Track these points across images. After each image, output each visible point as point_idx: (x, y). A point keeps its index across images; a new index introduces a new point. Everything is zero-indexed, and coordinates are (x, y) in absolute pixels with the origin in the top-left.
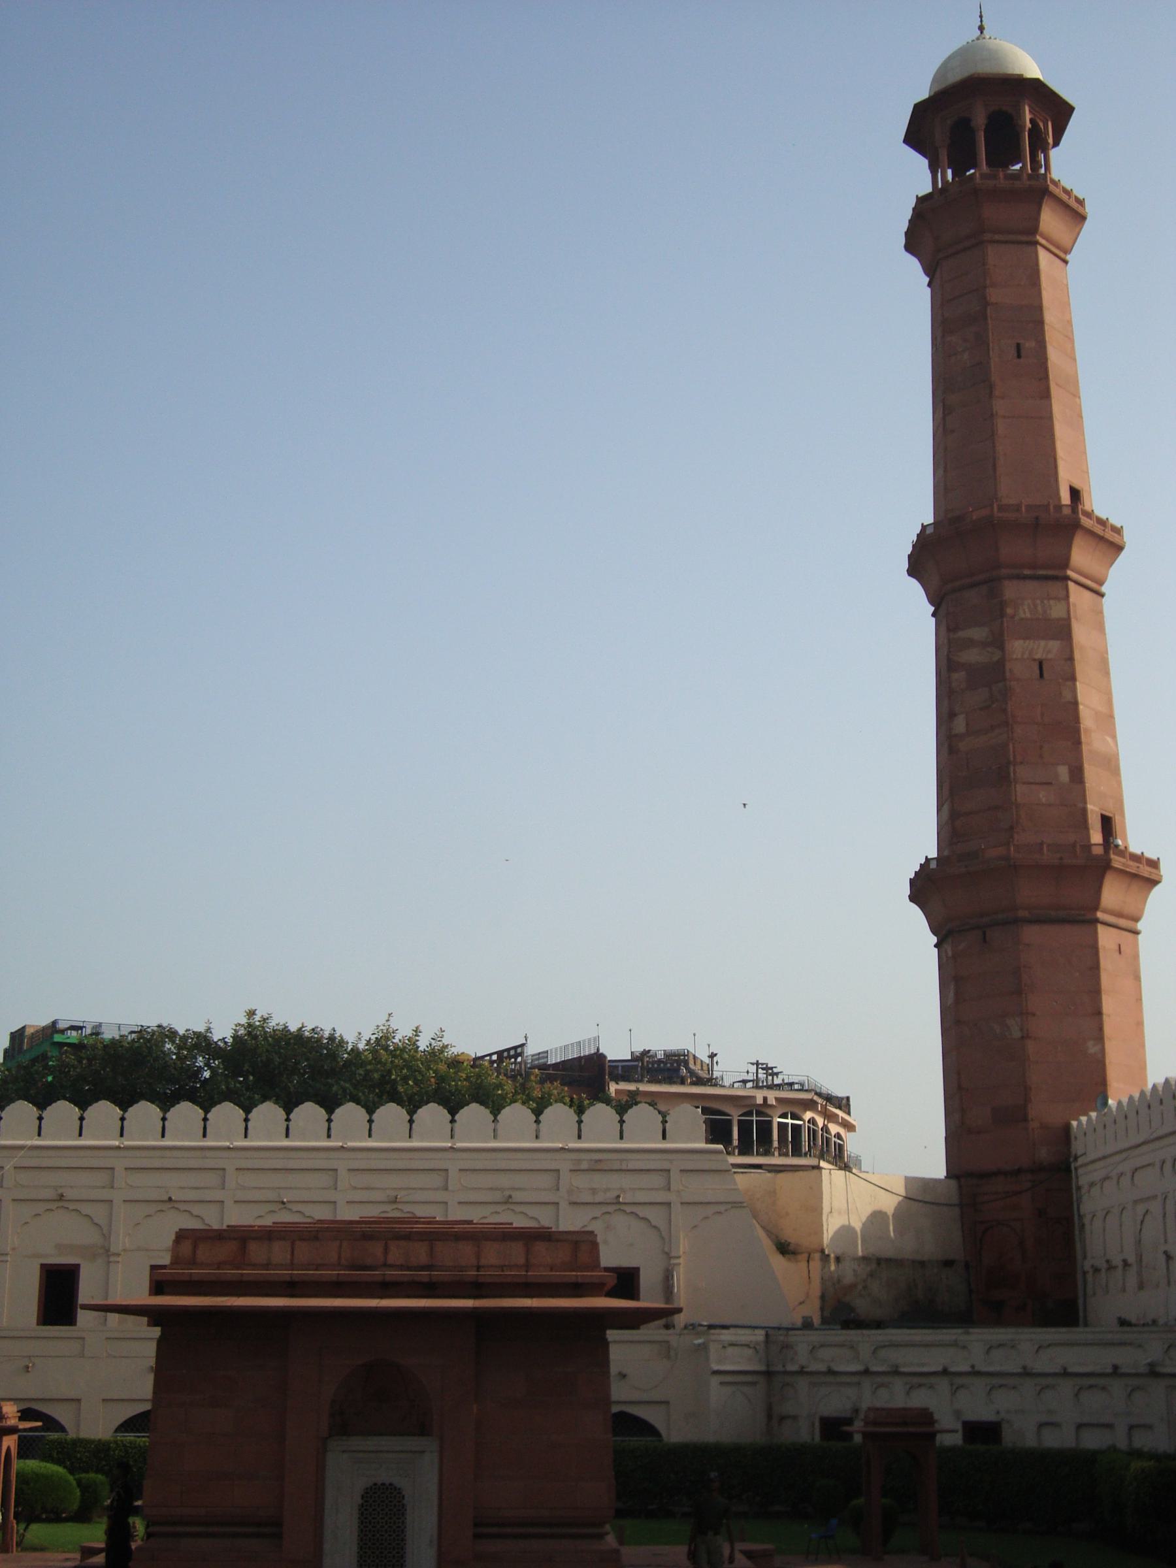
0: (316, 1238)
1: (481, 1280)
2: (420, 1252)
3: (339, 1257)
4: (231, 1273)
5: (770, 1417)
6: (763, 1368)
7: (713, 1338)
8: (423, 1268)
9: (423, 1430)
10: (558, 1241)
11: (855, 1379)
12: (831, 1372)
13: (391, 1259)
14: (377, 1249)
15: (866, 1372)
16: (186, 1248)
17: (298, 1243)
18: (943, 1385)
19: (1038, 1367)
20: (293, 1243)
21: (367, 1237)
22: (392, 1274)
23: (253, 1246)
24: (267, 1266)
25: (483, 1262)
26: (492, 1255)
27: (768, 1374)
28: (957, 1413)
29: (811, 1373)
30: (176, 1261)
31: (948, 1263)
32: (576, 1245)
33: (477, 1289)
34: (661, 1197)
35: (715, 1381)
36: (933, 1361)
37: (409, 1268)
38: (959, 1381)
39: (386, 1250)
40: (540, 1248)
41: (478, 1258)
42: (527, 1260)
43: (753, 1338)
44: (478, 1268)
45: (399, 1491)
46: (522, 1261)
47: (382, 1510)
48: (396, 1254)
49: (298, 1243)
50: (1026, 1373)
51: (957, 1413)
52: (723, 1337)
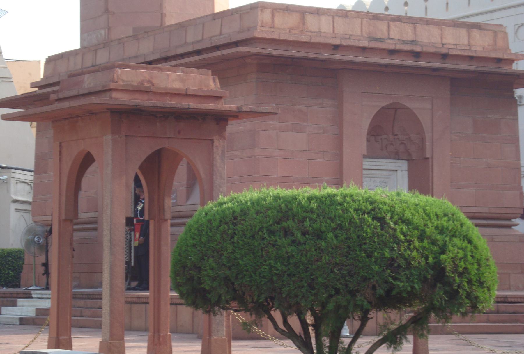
3: (362, 31)
7: (13, 175)
9: (396, 156)
10: (485, 30)
14: (382, 26)
17: (336, 19)
23: (309, 18)
24: (320, 32)
25: (445, 41)
32: (495, 32)
35: (14, 206)
39: (389, 27)
40: (476, 33)
42: (469, 41)
46: (466, 42)
49: (336, 19)
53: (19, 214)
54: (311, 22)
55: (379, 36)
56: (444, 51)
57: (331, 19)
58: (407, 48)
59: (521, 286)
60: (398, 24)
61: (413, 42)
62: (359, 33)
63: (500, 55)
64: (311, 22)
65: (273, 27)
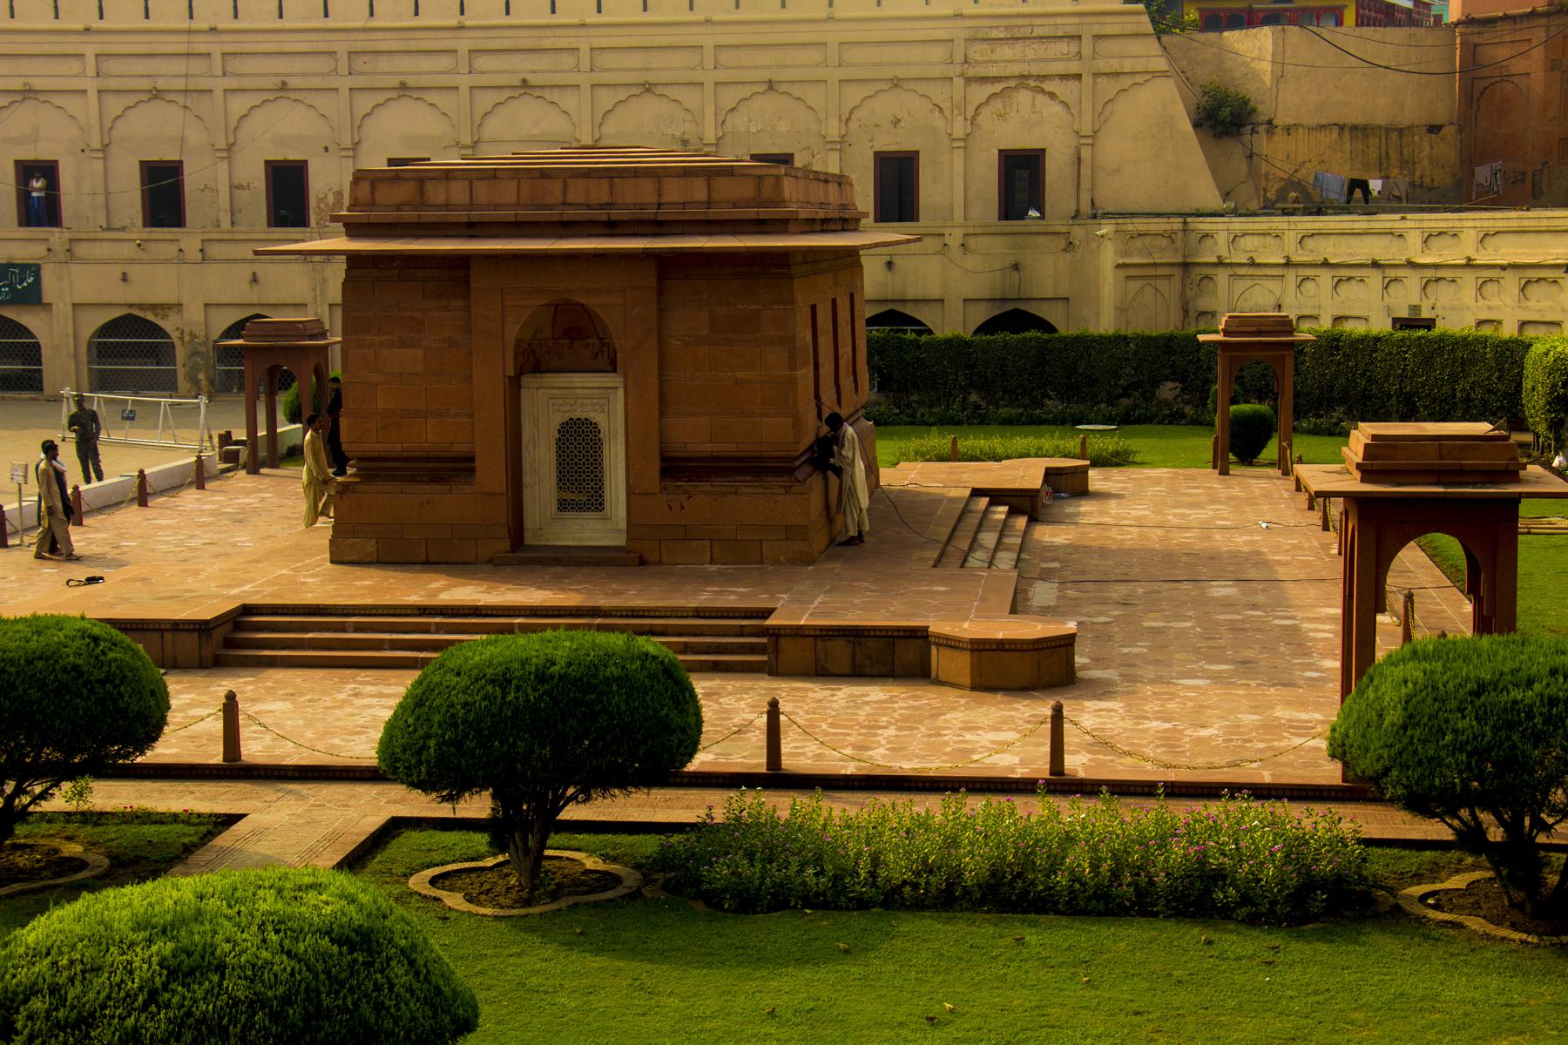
0: (495, 177)
1: (660, 218)
2: (600, 192)
4: (409, 215)
5: (1186, 312)
6: (1180, 260)
8: (602, 206)
11: (1280, 272)
12: (1253, 264)
13: (571, 198)
14: (556, 187)
15: (1288, 264)
16: (365, 188)
17: (475, 183)
18: (1374, 279)
19: (1481, 260)
20: (471, 182)
21: (544, 174)
22: (570, 214)
23: (430, 186)
24: (447, 206)
25: (665, 199)
26: (674, 192)
27: (1186, 266)
28: (1389, 309)
29: (1232, 265)
30: (354, 205)
31: (1434, 129)
33: (659, 227)
34: (1074, 67)
36: (1364, 250)
37: (589, 207)
38: (1392, 273)
40: (721, 182)
41: (660, 193)
43: (1168, 227)
44: (659, 205)
45: (595, 426)
46: (704, 197)
47: (579, 443)
48: (577, 193)
50: (1469, 265)
51: (1389, 309)
52: (1130, 227)
53: (1139, 284)
54: (436, 193)
55: (549, 200)
56: (649, 213)
57: (466, 184)
58: (602, 215)
59: (782, 559)
60: (582, 181)
61: (609, 206)
62: (514, 200)
63: (751, 213)
64: (436, 193)
65: (372, 204)
